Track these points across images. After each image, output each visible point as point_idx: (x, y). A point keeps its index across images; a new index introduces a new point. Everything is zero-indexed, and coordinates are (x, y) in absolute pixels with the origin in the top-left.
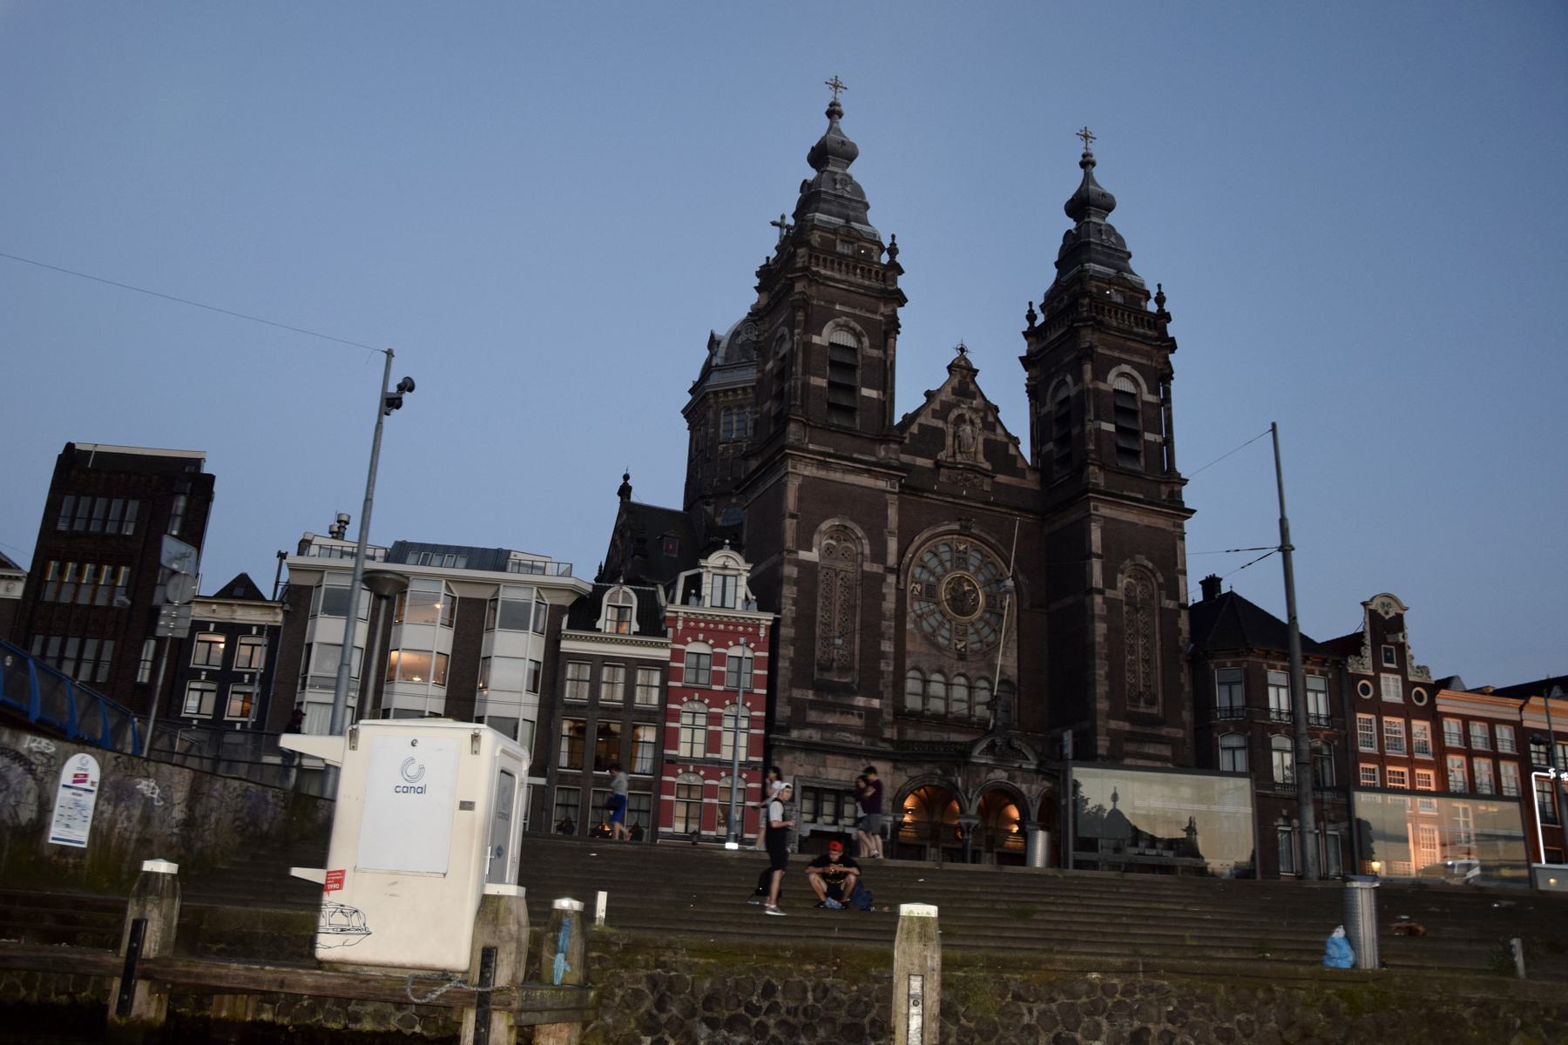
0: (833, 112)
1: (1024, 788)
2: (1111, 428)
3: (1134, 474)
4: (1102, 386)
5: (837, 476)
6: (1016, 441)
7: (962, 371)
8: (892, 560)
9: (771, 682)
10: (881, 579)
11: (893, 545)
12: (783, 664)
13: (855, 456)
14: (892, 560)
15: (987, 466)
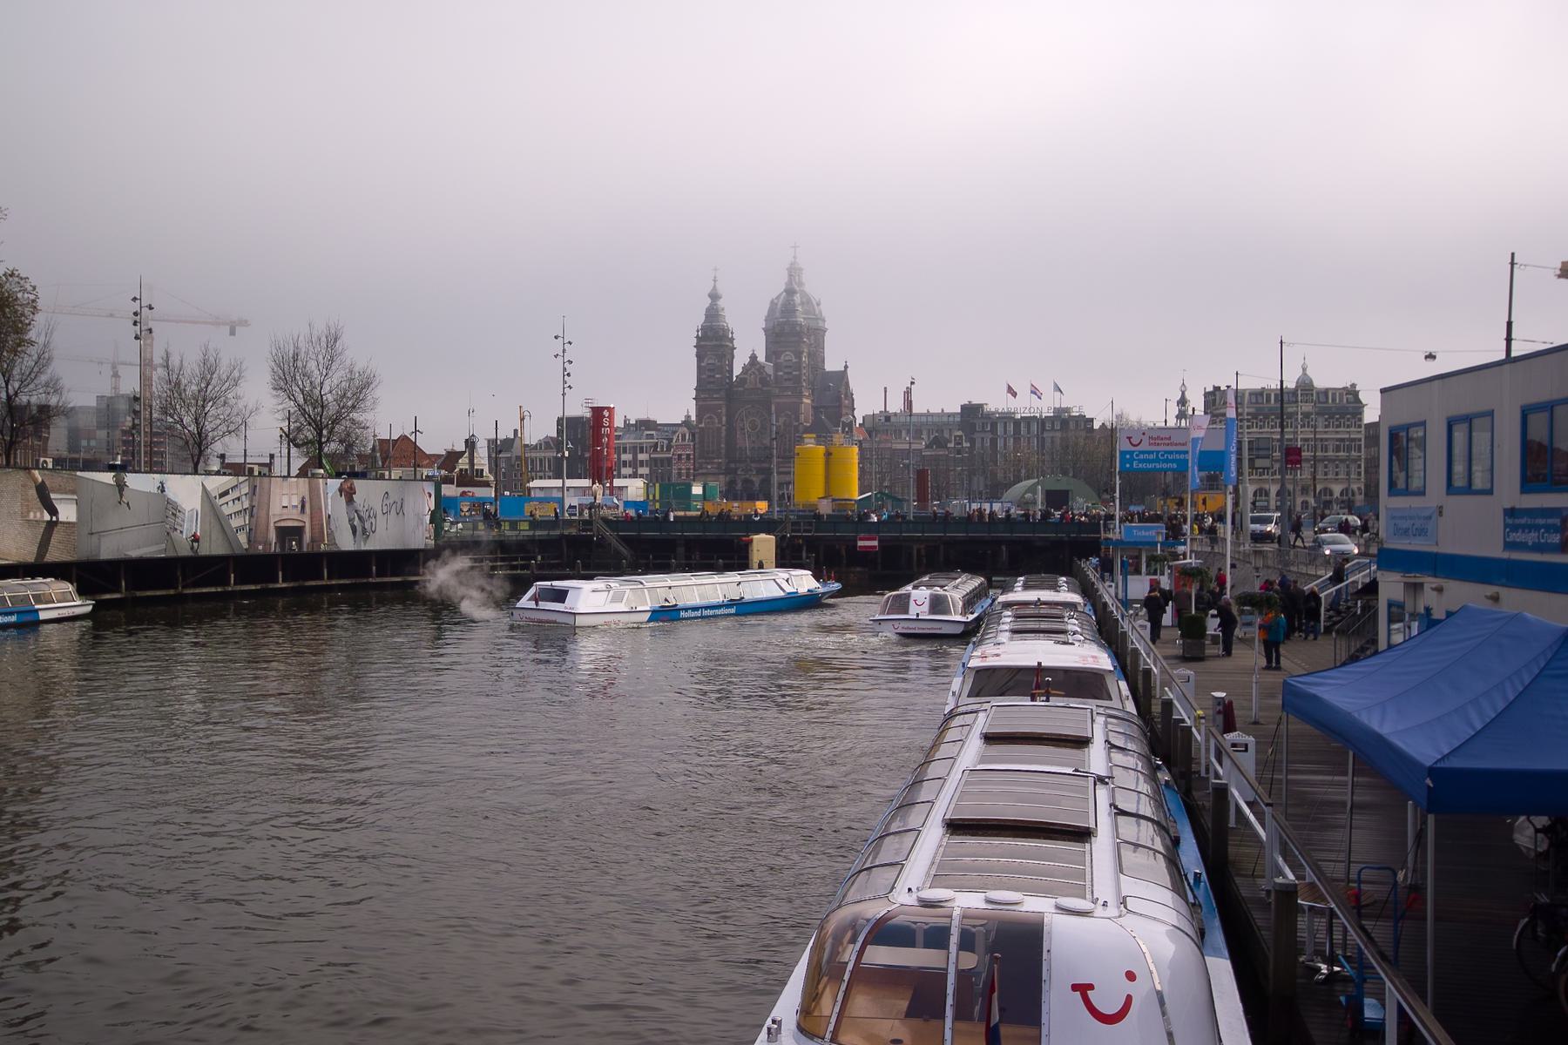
0: (715, 281)
1: (754, 479)
2: (781, 373)
3: (787, 388)
4: (778, 361)
5: (709, 403)
6: (770, 376)
7: (753, 358)
8: (724, 423)
9: (694, 458)
10: (720, 428)
11: (724, 419)
12: (696, 455)
13: (715, 396)
14: (724, 423)
15: (759, 386)
